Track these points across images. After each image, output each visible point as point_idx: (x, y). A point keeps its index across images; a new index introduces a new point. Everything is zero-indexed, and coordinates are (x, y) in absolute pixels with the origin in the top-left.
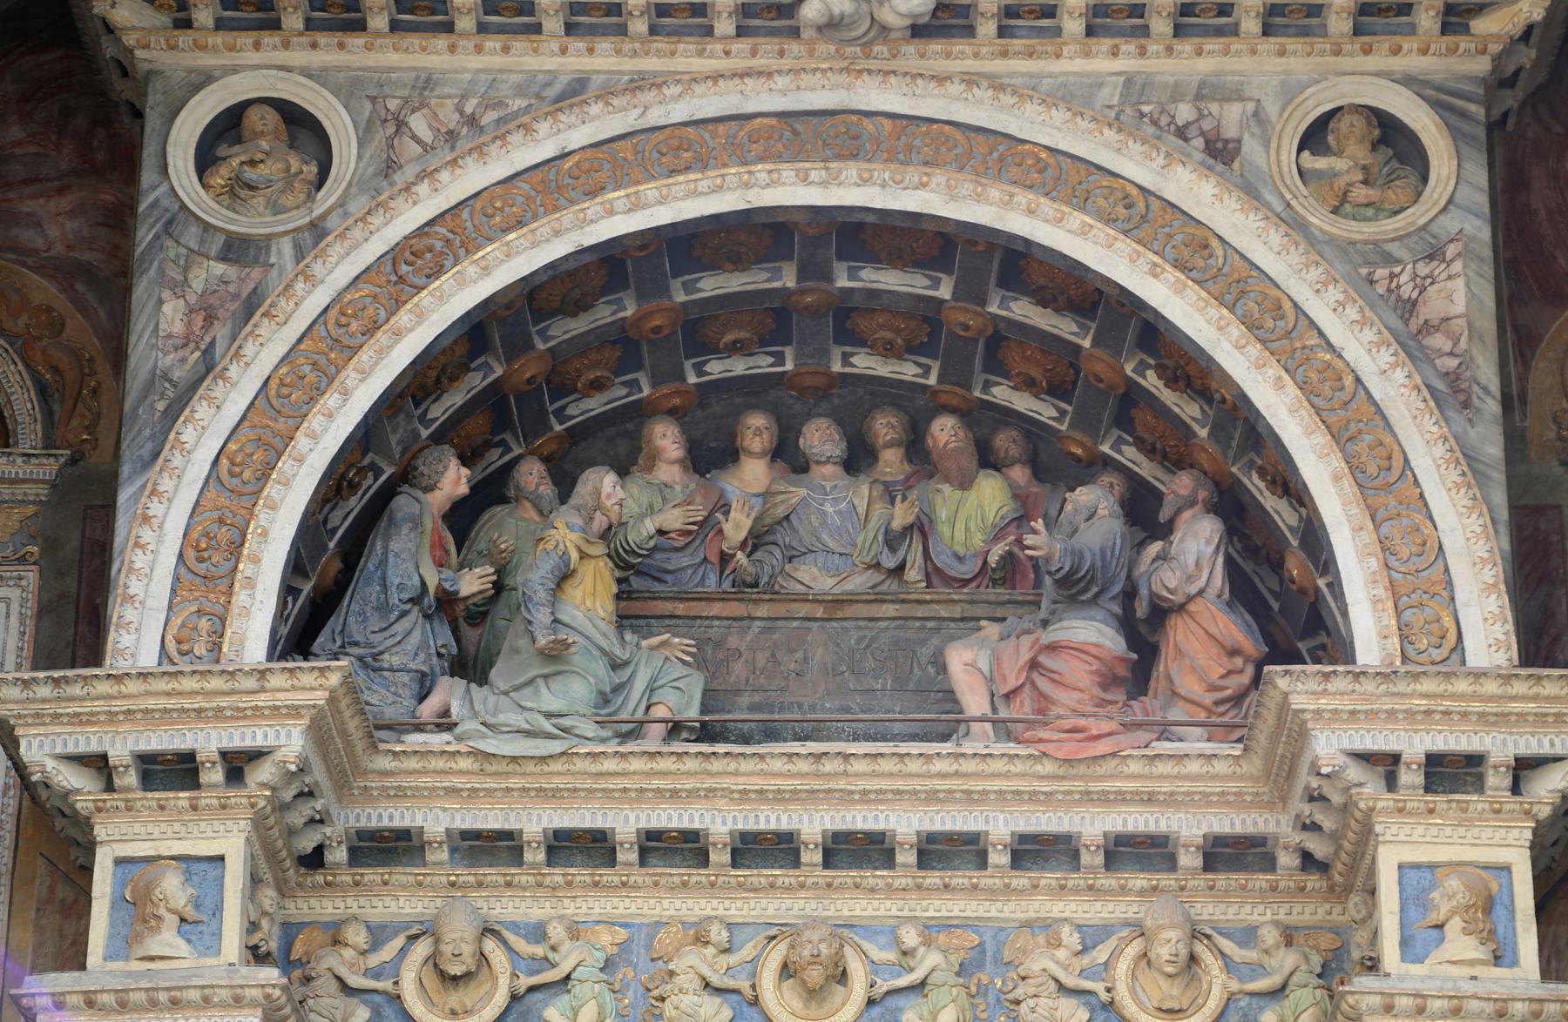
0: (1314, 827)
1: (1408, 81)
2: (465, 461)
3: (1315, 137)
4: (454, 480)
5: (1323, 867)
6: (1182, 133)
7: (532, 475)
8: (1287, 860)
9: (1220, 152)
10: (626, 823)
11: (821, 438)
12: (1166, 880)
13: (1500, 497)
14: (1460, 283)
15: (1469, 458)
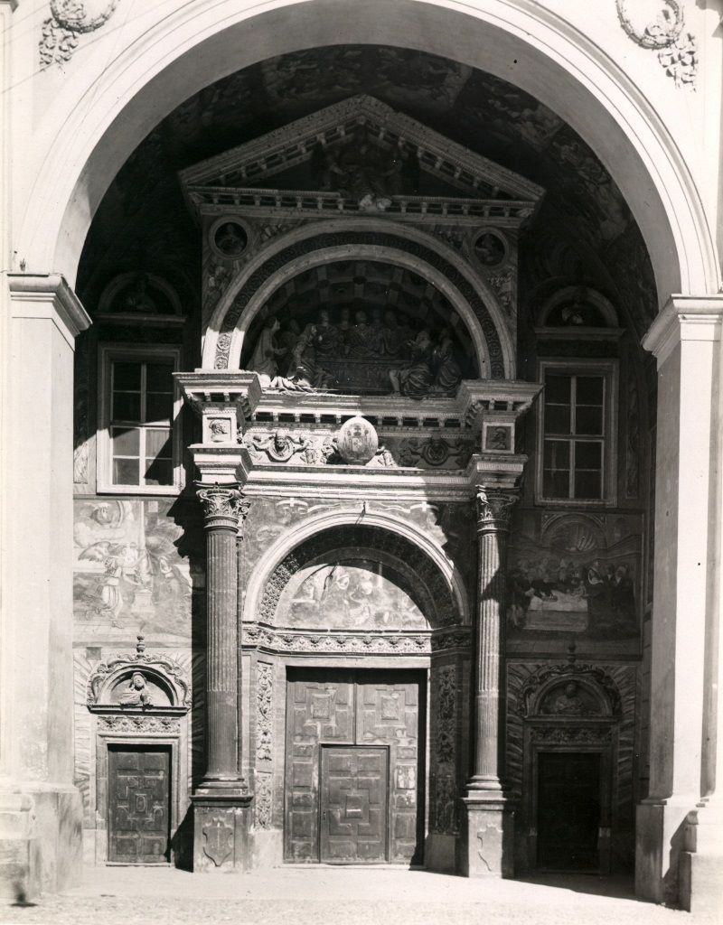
0: (468, 417)
1: (501, 229)
2: (279, 320)
3: (479, 243)
4: (276, 326)
5: (470, 426)
6: (448, 240)
7: (294, 324)
8: (463, 425)
9: (457, 246)
10: (318, 413)
11: (360, 316)
12: (437, 429)
13: (515, 339)
14: (510, 283)
15: (509, 329)
